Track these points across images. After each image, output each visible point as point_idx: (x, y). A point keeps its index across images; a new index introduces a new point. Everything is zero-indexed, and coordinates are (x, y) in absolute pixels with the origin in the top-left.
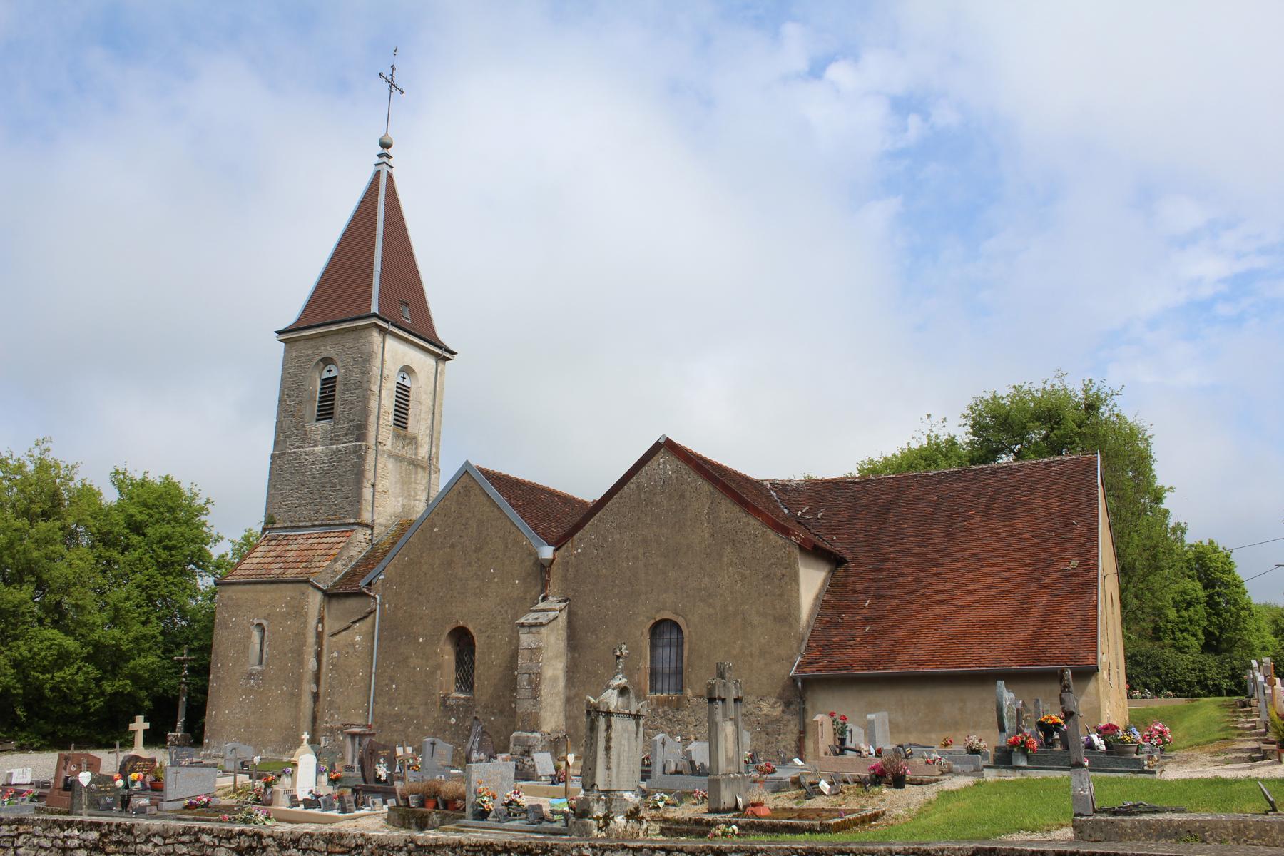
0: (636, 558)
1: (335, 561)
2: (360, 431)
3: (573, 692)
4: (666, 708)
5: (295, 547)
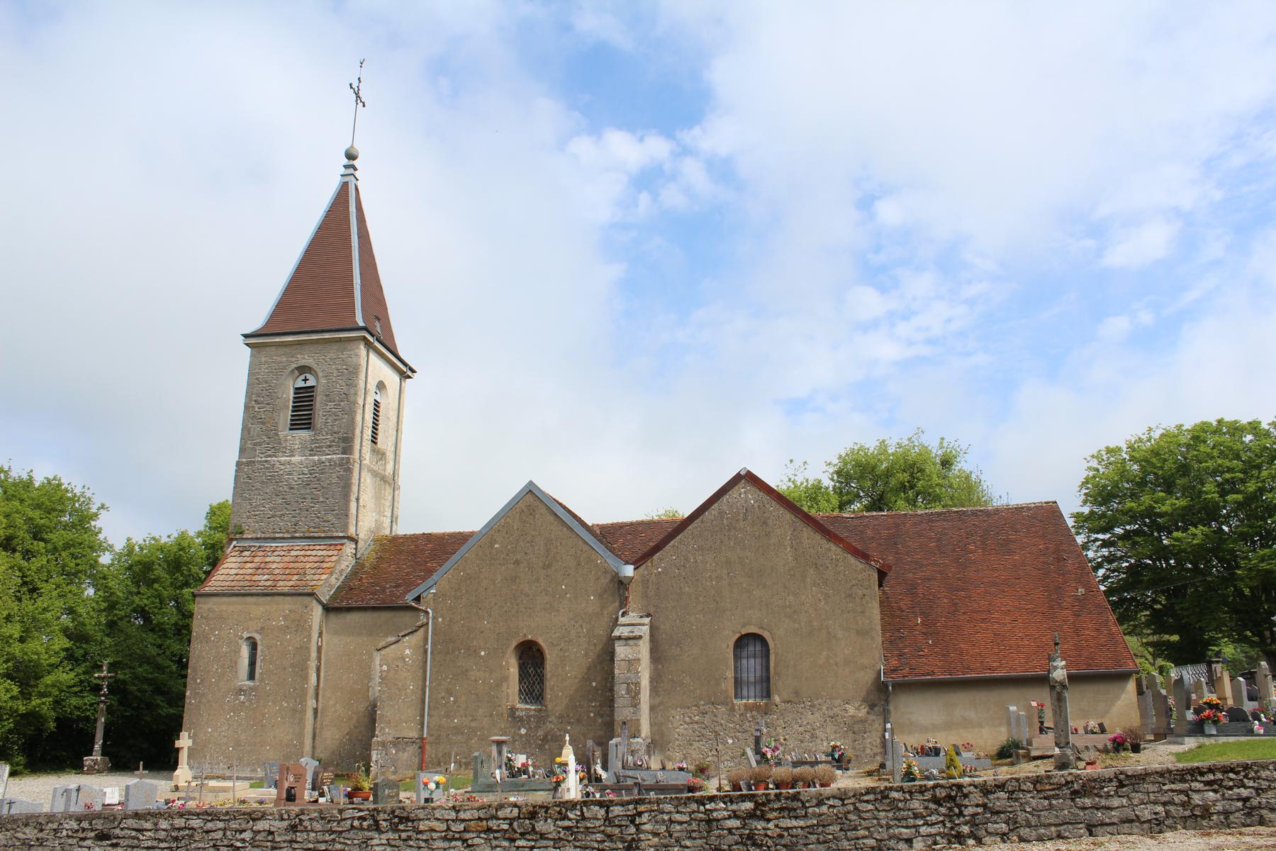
0: (719, 578)
1: (331, 574)
2: (346, 444)
3: (657, 700)
4: (754, 713)
5: (278, 559)
